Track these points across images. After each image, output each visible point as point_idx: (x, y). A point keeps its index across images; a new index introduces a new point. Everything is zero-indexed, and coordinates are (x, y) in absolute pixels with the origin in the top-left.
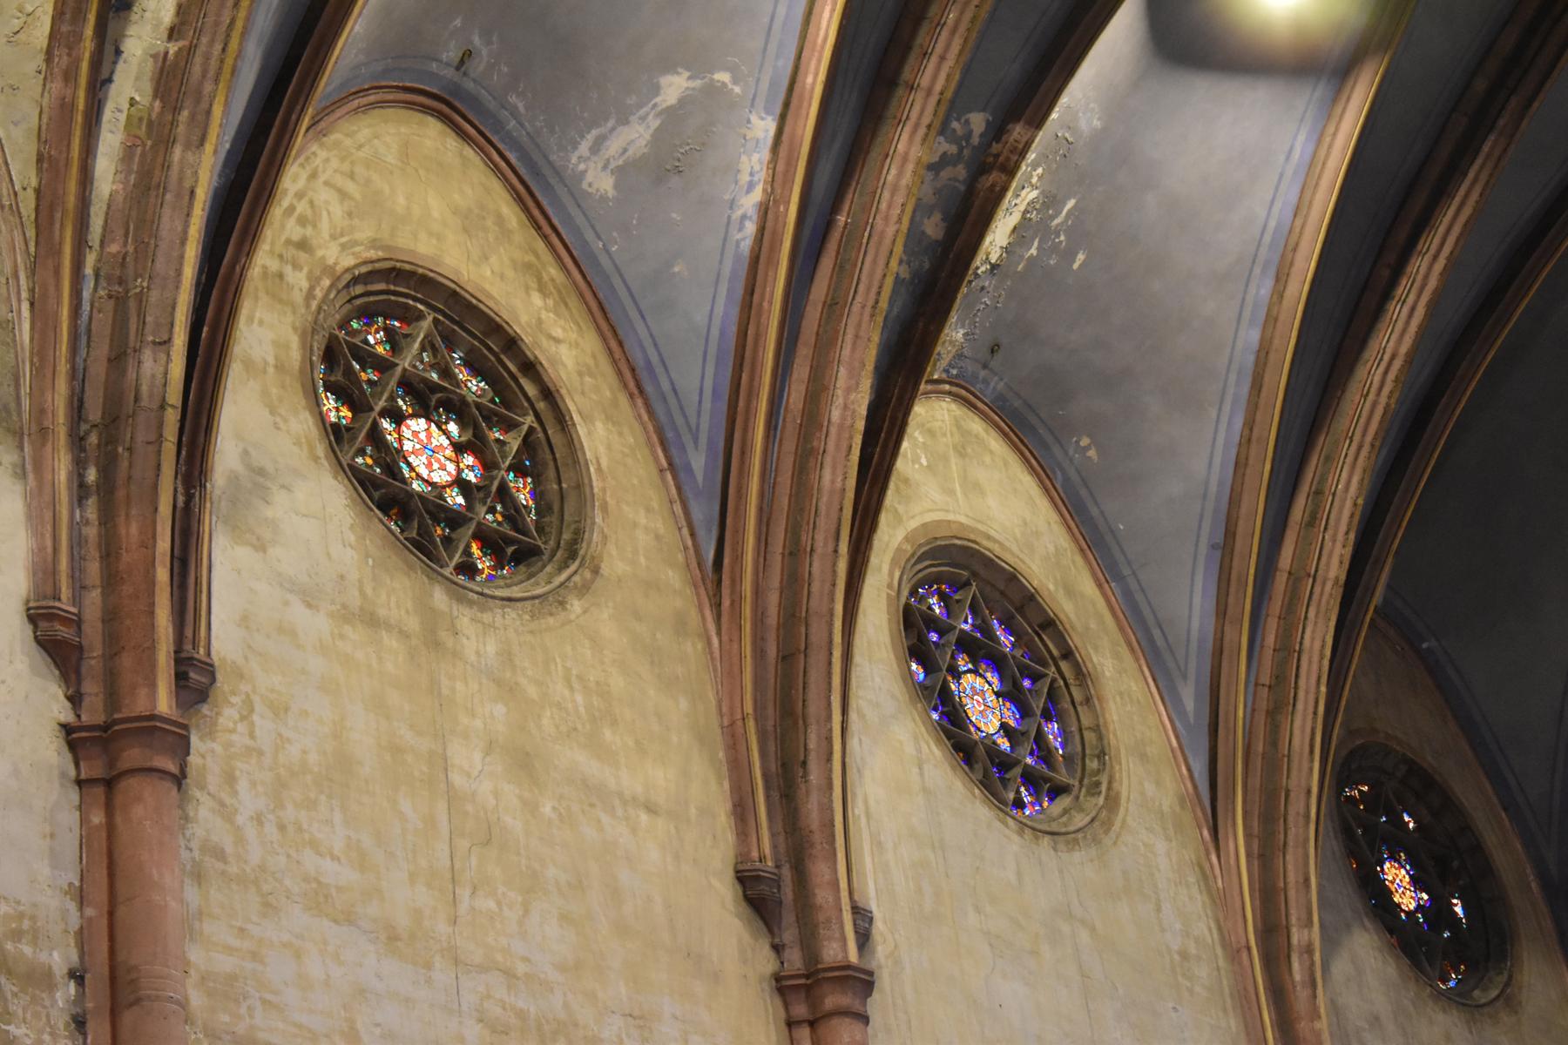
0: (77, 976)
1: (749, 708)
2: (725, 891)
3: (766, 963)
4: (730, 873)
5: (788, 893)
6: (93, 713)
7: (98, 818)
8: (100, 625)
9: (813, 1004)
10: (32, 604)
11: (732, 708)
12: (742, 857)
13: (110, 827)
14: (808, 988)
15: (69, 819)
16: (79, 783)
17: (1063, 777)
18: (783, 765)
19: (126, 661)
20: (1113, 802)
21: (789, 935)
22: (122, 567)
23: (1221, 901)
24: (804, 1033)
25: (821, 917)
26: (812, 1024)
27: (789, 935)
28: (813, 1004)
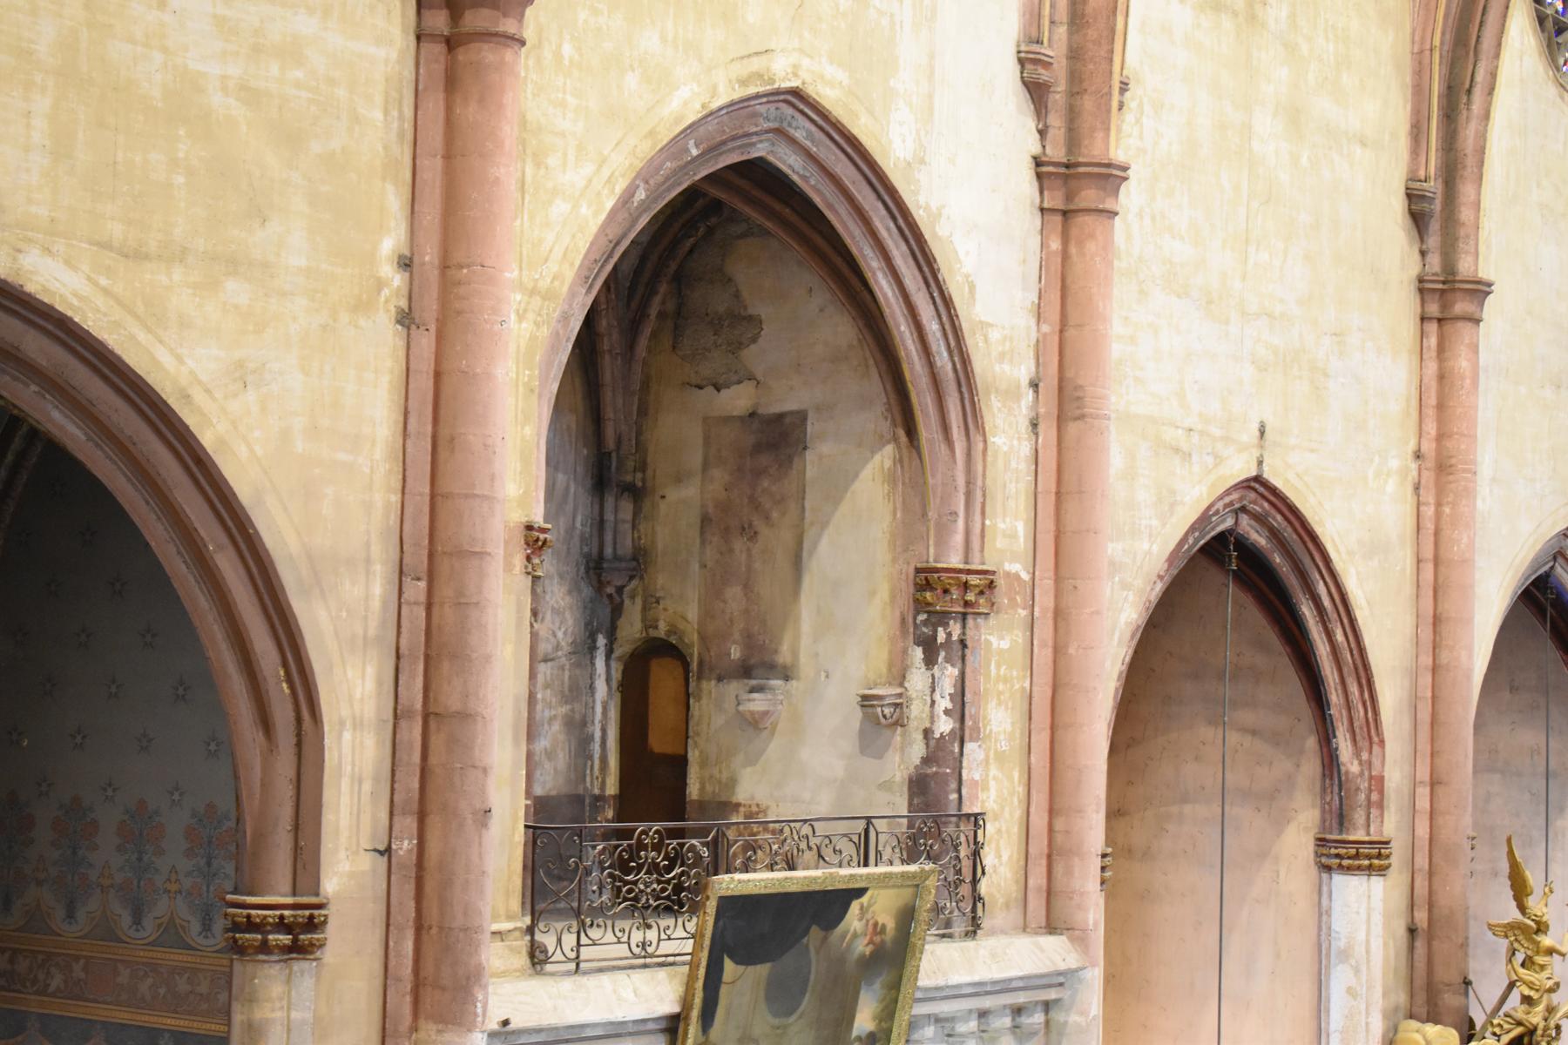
1: (1437, 42)
2: (1397, 205)
3: (1414, 268)
4: (1402, 191)
5: (1437, 206)
6: (1056, 152)
7: (1055, 245)
8: (1064, 61)
9: (1445, 306)
10: (1023, 48)
11: (1423, 39)
12: (1412, 178)
13: (1065, 255)
14: (1443, 291)
16: (1042, 210)
18: (1449, 87)
19: (1088, 103)
21: (1433, 241)
22: (1089, 10)
24: (1432, 328)
25: (1462, 232)
27: (1433, 241)
28: (1445, 306)
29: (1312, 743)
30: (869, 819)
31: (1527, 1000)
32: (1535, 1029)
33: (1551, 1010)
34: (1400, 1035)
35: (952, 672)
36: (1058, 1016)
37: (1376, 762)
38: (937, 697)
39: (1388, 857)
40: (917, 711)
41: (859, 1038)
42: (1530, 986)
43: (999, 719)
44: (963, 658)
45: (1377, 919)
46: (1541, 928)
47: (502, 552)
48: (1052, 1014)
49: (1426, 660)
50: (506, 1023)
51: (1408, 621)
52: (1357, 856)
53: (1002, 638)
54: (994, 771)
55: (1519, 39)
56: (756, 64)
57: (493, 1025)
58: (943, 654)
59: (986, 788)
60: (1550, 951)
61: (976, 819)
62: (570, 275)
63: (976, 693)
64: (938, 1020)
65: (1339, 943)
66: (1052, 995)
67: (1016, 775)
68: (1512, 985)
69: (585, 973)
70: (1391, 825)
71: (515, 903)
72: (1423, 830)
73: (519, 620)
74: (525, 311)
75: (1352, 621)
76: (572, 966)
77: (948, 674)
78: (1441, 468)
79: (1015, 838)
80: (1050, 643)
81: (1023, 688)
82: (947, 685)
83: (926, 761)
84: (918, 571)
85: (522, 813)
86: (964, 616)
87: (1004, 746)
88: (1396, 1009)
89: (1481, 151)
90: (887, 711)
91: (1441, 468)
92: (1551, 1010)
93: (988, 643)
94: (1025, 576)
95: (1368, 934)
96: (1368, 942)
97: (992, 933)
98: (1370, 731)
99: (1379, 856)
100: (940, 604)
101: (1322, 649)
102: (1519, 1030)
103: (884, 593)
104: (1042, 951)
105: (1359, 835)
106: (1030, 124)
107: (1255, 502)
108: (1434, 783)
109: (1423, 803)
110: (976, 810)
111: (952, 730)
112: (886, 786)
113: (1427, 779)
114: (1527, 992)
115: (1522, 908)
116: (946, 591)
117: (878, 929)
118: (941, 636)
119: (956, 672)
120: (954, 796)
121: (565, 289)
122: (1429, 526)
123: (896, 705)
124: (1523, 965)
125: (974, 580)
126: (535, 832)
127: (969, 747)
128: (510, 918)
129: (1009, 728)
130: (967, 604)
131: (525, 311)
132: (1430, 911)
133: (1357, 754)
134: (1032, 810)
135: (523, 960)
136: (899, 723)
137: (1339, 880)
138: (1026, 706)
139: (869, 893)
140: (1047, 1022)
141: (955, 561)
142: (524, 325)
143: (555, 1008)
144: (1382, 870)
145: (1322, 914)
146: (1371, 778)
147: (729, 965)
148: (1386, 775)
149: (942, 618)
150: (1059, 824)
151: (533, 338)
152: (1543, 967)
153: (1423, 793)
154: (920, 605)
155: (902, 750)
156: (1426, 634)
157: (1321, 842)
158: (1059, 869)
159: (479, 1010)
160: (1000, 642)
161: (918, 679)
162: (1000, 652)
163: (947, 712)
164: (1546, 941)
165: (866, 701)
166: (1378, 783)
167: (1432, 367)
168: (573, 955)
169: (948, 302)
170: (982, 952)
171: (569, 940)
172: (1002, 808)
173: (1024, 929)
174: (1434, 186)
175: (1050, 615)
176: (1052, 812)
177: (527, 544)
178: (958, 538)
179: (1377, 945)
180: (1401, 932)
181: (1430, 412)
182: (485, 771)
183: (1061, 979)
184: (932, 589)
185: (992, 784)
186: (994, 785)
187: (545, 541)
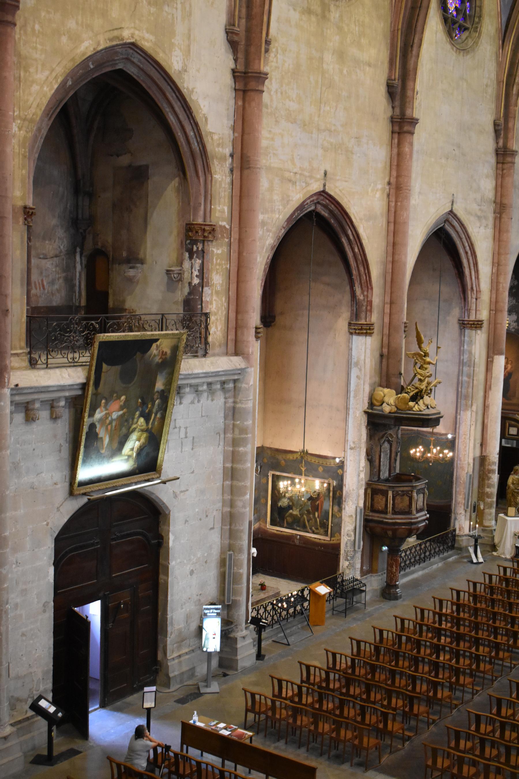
0: (232, 156)
1: (400, 27)
2: (383, 89)
3: (389, 113)
4: (385, 83)
5: (399, 90)
6: (241, 68)
7: (240, 103)
8: (244, 33)
9: (401, 128)
10: (228, 27)
11: (395, 25)
12: (389, 79)
13: (244, 108)
14: (400, 122)
15: (232, 102)
16: (235, 90)
17: (468, 25)
18: (405, 45)
19: (253, 49)
20: (480, 34)
21: (397, 103)
22: (253, 13)
23: (499, 65)
24: (396, 136)
25: (408, 100)
26: (399, 133)
27: (397, 103)
28: (401, 128)
29: (348, 288)
30: (163, 315)
31: (420, 380)
32: (422, 390)
33: (429, 384)
34: (376, 392)
35: (199, 261)
36: (239, 385)
37: (370, 295)
38: (193, 270)
39: (373, 329)
40: (186, 275)
41: (158, 392)
42: (421, 375)
43: (217, 279)
44: (203, 257)
45: (368, 352)
46: (426, 355)
47: (11, 217)
48: (237, 384)
49: (390, 259)
50: (17, 385)
51: (384, 244)
52: (361, 329)
53: (218, 249)
54: (214, 297)
55: (433, 27)
56: (116, 33)
57: (12, 386)
58: (195, 255)
59: (211, 303)
60: (429, 363)
61: (207, 315)
62: (40, 113)
63: (208, 269)
64: (191, 386)
65: (354, 360)
66: (236, 377)
67: (224, 299)
68: (415, 376)
69: (50, 368)
70: (374, 318)
71: (23, 344)
72: (387, 320)
73: (22, 242)
74: (22, 127)
75: (361, 244)
76: (45, 366)
77: (198, 262)
78: (397, 189)
79: (223, 322)
80: (237, 252)
81: (226, 268)
82: (197, 266)
83: (189, 294)
84: (187, 224)
85: (25, 311)
86: (203, 242)
87: (219, 288)
88: (375, 383)
89: (415, 69)
90: (175, 276)
91: (397, 189)
92: (429, 384)
93: (213, 251)
94: (228, 227)
95: (365, 356)
96: (365, 360)
97: (214, 355)
98: (368, 285)
99: (370, 329)
100: (195, 237)
101: (350, 254)
102: (417, 390)
103: (175, 232)
104: (231, 361)
105: (363, 322)
106: (231, 57)
107: (323, 200)
108: (391, 303)
109: (387, 310)
110: (208, 311)
111: (199, 283)
112: (176, 303)
113: (389, 301)
114: (420, 377)
115: (420, 347)
116: (197, 232)
117: (164, 354)
118: (195, 248)
119: (200, 262)
120: (199, 306)
121: (38, 118)
122: (393, 210)
123: (179, 274)
124: (420, 368)
125: (207, 228)
126: (30, 319)
127: (206, 289)
128: (21, 348)
129: (221, 282)
130: (204, 237)
131: (22, 127)
132: (388, 349)
133: (363, 292)
134: (230, 311)
135: (26, 363)
136: (181, 280)
137: (355, 337)
138: (228, 274)
139: (160, 341)
140: (235, 387)
141: (200, 221)
142: (21, 132)
143: (37, 380)
144: (371, 334)
146: (368, 301)
147: (105, 366)
148: (373, 300)
149: (195, 242)
150: (239, 317)
151: (25, 137)
152: (426, 369)
153: (387, 307)
154: (187, 237)
155: (181, 289)
156: (390, 248)
157: (350, 324)
158: (239, 333)
159: (6, 380)
160: (218, 251)
161: (187, 264)
162: (218, 254)
163: (197, 276)
164: (428, 359)
165: (168, 272)
166: (370, 303)
167: (395, 151)
168: (45, 362)
169: (197, 124)
170: (207, 362)
171: (44, 358)
172: (218, 311)
173: (227, 354)
174: (397, 83)
175: (237, 241)
176: (237, 312)
177: (25, 213)
178: (201, 213)
179: (368, 361)
180: (377, 355)
181: (394, 167)
182: (6, 296)
183: (242, 372)
184: (192, 231)
185: (214, 302)
186: (215, 304)
187: (32, 213)
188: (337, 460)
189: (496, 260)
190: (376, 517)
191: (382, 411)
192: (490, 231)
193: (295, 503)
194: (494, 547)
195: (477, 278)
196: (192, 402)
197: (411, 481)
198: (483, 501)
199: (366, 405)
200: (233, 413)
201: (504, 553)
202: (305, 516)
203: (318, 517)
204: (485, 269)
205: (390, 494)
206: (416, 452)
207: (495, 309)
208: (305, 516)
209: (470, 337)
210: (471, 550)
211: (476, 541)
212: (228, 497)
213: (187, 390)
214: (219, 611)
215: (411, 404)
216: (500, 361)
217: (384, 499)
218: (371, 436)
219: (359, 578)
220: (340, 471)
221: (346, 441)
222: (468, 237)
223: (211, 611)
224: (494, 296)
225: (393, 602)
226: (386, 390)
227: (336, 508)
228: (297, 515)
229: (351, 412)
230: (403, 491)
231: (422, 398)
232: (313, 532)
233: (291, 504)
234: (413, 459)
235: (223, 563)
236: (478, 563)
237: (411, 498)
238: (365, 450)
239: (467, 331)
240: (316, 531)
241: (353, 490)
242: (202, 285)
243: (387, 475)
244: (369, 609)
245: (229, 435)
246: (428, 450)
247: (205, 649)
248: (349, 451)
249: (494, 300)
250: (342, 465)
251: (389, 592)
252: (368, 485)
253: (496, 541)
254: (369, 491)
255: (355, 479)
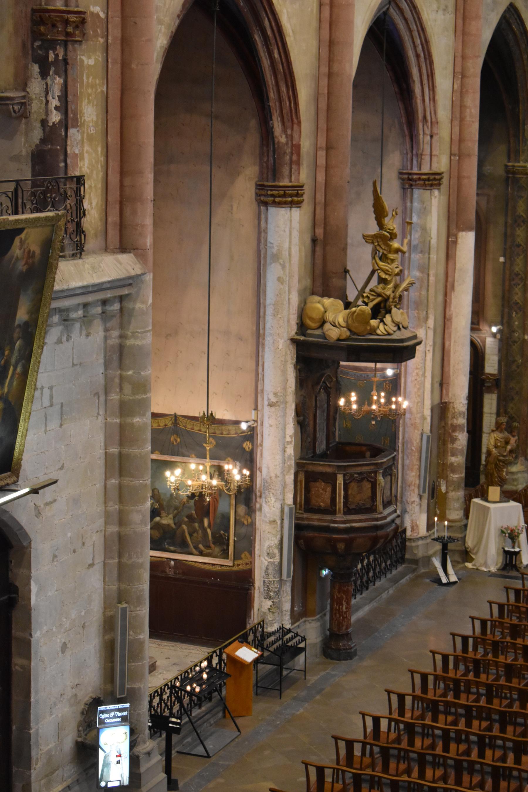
29: (253, 123)
30: (17, 182)
32: (388, 297)
33: (396, 287)
34: (309, 305)
35: (59, 80)
36: (128, 305)
37: (296, 136)
38: (50, 98)
39: (302, 195)
40: (36, 107)
41: (19, 326)
42: (386, 272)
43: (89, 113)
44: (66, 71)
45: (296, 234)
48: (125, 304)
49: (325, 69)
51: (314, 43)
52: (284, 195)
53: (89, 58)
54: (86, 148)
58: (53, 69)
59: (82, 159)
61: (80, 180)
63: (75, 95)
64: (60, 311)
66: (126, 291)
67: (99, 149)
68: (373, 272)
70: (304, 176)
72: (321, 177)
77: (57, 83)
79: (99, 191)
80: (119, 61)
81: (102, 91)
82: (56, 90)
83: (43, 141)
84: (34, 11)
87: (92, 131)
88: (305, 289)
90: (16, 108)
93: (82, 61)
94: (102, 15)
95: (290, 242)
96: (290, 248)
97: (88, 253)
98: (292, 117)
99: (297, 195)
101: (266, 63)
102: (379, 299)
103: (9, 26)
104: (121, 263)
105: (285, 182)
108: (329, 148)
109: (322, 161)
110: (77, 174)
111: (60, 121)
112: (16, 158)
113: (324, 145)
114: (383, 276)
115: (381, 225)
116: (54, 26)
117: (30, 255)
118: (51, 56)
119: (62, 81)
120: (62, 164)
123: (22, 104)
124: (380, 259)
125: (72, 18)
127: (72, 131)
129: (95, 119)
130: (68, 34)
132: (325, 228)
133: (285, 131)
134: (110, 172)
136: (24, 114)
137: (272, 210)
138: (104, 104)
139: (25, 231)
140: (121, 309)
144: (298, 204)
145: (261, 233)
146: (292, 145)
148: (302, 143)
149: (52, 44)
150: (127, 182)
152: (393, 261)
153: (322, 154)
154: (36, 35)
155: (26, 135)
157: (260, 187)
158: (128, 211)
160: (89, 59)
161: (36, 87)
162: (89, 66)
163: (56, 108)
164: (396, 244)
170: (87, 266)
172: (92, 171)
173: (106, 250)
175: (119, 42)
176: (123, 173)
179: (295, 250)
184: (44, 24)
185: (86, 155)
186: (86, 158)
188: (244, 426)
189: (458, 69)
190: (316, 519)
191: (324, 336)
192: (450, 17)
193: (165, 503)
194: (466, 555)
195: (433, 99)
196: (59, 341)
197: (362, 456)
198: (446, 478)
199: (294, 329)
200: (120, 356)
201: (485, 564)
202: (185, 527)
203: (209, 526)
204: (444, 83)
205: (340, 479)
206: (348, 402)
207: (458, 155)
208: (185, 527)
209: (422, 202)
210: (437, 563)
211: (445, 547)
212: (114, 507)
213: (56, 319)
214: (125, 713)
215: (374, 322)
216: (467, 241)
217: (329, 489)
218: (301, 382)
219: (288, 626)
220: (247, 446)
221: (257, 392)
222: (422, 29)
223: (112, 714)
224: (456, 129)
225: (344, 664)
226: (327, 301)
227: (242, 509)
228: (169, 525)
229: (268, 340)
230: (360, 474)
231: (389, 311)
232: (201, 554)
233: (157, 506)
234: (347, 415)
235: (108, 625)
236: (450, 584)
237: (374, 485)
238: (293, 406)
239: (417, 193)
240: (206, 551)
241: (276, 476)
242: (65, 124)
243: (323, 446)
244: (312, 679)
245: (114, 397)
246: (365, 398)
247: (103, 784)
248: (267, 410)
249: (456, 137)
250: (251, 435)
251: (337, 646)
252: (299, 466)
253: (470, 543)
254: (302, 476)
255: (279, 457)
